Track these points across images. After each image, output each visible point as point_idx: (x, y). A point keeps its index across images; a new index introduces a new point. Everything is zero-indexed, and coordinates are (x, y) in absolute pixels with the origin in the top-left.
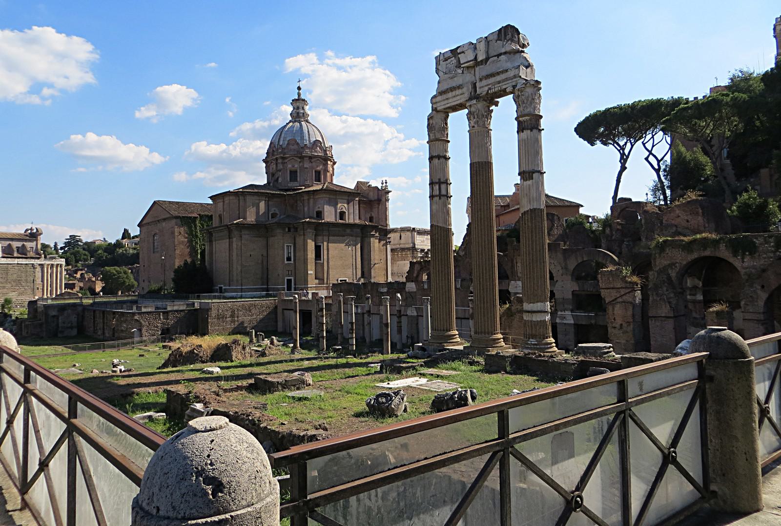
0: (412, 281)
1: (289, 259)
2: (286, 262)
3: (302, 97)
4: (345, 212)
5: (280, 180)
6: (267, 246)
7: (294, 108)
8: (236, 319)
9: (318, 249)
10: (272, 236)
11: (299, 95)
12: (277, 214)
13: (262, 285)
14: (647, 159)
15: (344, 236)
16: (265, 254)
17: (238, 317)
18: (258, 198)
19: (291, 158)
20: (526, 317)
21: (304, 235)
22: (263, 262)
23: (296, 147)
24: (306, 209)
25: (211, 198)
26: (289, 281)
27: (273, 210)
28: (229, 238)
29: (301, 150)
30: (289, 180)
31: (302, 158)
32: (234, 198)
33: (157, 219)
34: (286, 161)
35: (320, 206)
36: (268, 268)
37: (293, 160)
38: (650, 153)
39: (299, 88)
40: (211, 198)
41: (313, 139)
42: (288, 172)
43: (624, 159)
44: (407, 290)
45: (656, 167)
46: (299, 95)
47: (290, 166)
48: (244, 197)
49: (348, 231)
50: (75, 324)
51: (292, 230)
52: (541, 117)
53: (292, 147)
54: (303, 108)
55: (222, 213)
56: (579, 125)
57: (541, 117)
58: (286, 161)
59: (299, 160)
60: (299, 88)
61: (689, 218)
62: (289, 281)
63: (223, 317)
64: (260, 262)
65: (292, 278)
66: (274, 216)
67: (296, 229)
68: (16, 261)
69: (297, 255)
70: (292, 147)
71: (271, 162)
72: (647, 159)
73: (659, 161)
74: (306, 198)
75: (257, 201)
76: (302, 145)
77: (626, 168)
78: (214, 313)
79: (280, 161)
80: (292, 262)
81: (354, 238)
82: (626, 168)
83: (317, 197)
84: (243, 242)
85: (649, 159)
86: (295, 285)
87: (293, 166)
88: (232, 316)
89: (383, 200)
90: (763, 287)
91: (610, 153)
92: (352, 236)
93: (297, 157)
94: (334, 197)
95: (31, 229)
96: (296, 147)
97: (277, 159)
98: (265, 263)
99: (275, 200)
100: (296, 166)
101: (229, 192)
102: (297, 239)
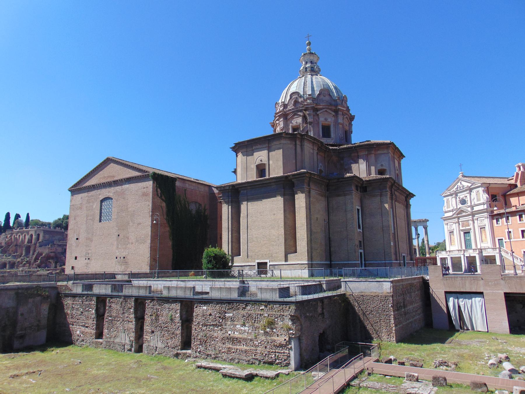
2: (359, 230)
13: (326, 261)
18: (312, 147)
19: (325, 110)
21: (381, 195)
32: (289, 142)
33: (109, 180)
36: (329, 238)
47: (322, 119)
55: (265, 161)
58: (318, 113)
65: (362, 251)
71: (294, 115)
80: (361, 231)
83: (379, 152)
84: (311, 199)
87: (326, 119)
93: (331, 109)
100: (329, 120)
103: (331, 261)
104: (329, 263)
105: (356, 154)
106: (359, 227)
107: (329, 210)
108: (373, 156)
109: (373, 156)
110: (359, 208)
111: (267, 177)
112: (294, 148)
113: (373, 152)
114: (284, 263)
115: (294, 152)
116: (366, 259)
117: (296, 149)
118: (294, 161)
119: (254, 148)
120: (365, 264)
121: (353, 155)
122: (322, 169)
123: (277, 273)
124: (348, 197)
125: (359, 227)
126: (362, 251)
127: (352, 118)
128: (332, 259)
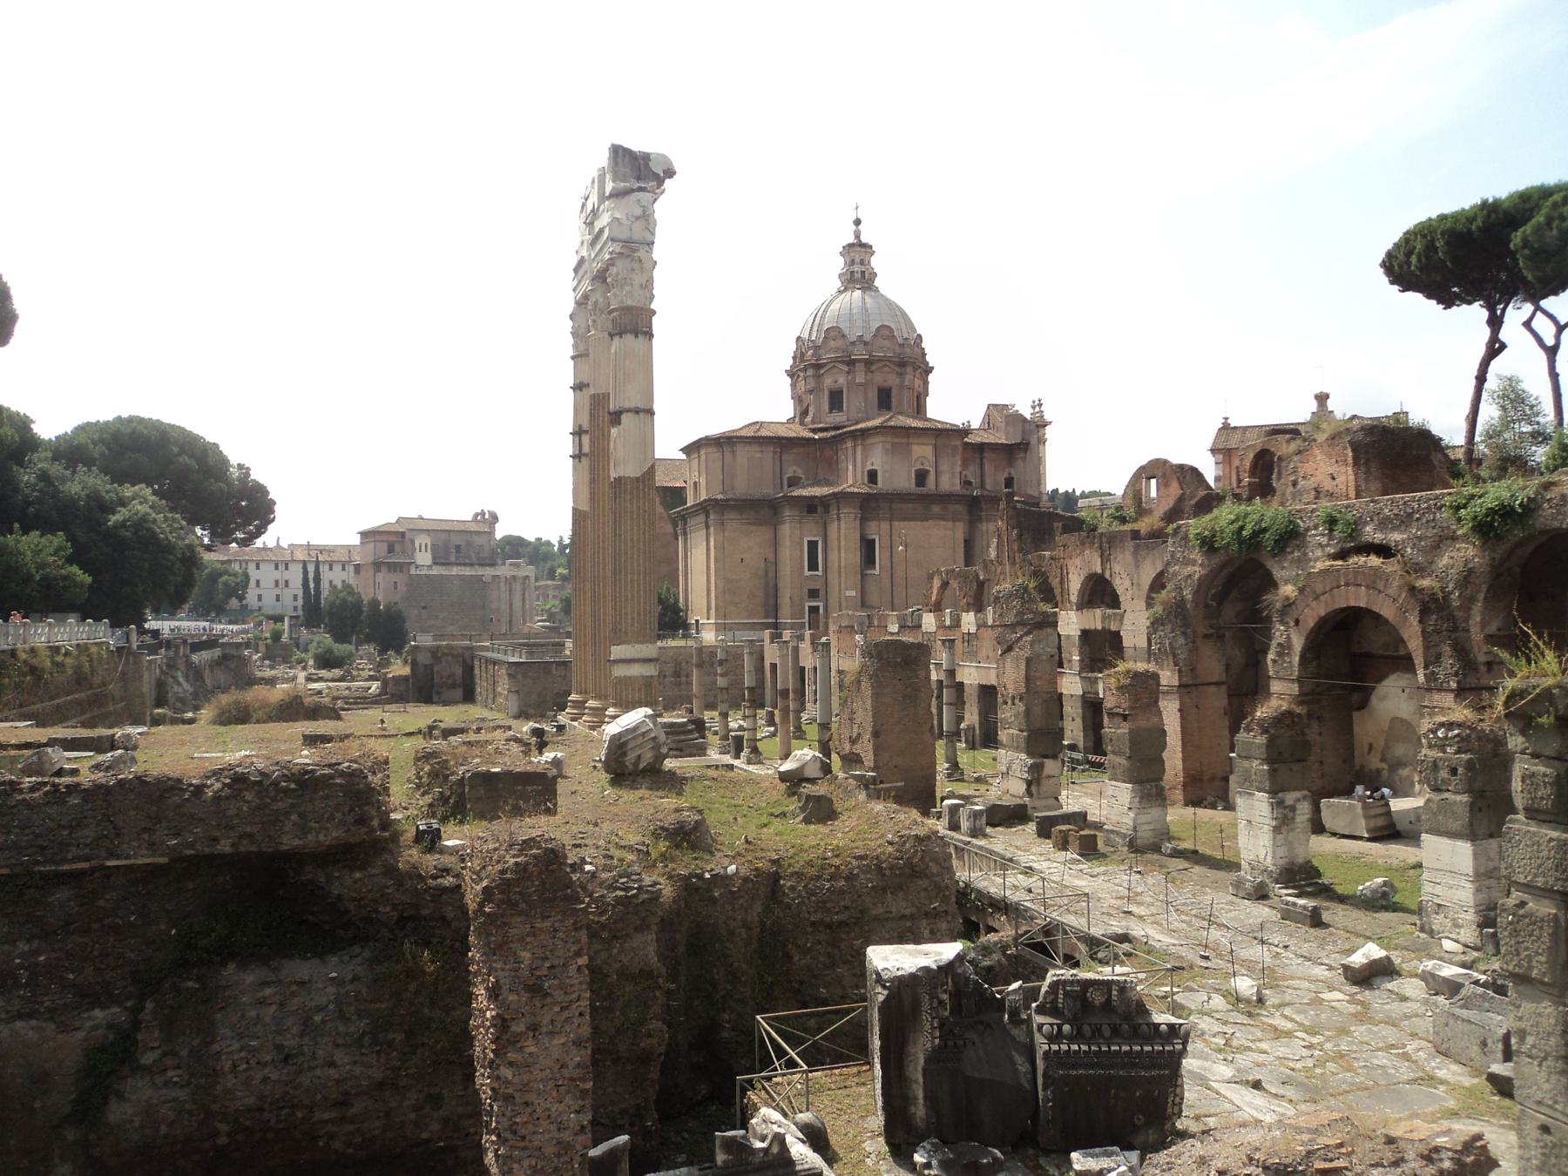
2: (807, 573)
3: (864, 239)
4: (927, 472)
6: (775, 543)
7: (853, 262)
9: (868, 547)
11: (857, 236)
14: (1527, 324)
16: (771, 558)
20: (619, 671)
21: (839, 519)
22: (766, 573)
26: (814, 610)
27: (792, 470)
30: (826, 408)
31: (851, 363)
38: (1538, 308)
39: (857, 222)
41: (875, 325)
42: (826, 393)
43: (1495, 322)
44: (924, 629)
45: (1550, 342)
46: (857, 236)
47: (828, 382)
49: (936, 509)
50: (459, 681)
51: (820, 509)
52: (654, 313)
53: (832, 344)
54: (862, 263)
56: (1389, 255)
57: (654, 313)
60: (857, 222)
61: (1333, 469)
64: (761, 573)
68: (455, 571)
70: (832, 344)
72: (1527, 324)
73: (1560, 328)
74: (849, 444)
75: (758, 455)
76: (853, 339)
77: (1503, 346)
80: (820, 573)
81: (950, 524)
82: (1503, 346)
83: (869, 441)
85: (1534, 324)
89: (1033, 441)
90: (1297, 622)
91: (1474, 315)
92: (943, 519)
95: (483, 513)
96: (839, 343)
98: (771, 575)
102: (833, 528)
106: (813, 566)
122: (800, 473)
125: (813, 566)
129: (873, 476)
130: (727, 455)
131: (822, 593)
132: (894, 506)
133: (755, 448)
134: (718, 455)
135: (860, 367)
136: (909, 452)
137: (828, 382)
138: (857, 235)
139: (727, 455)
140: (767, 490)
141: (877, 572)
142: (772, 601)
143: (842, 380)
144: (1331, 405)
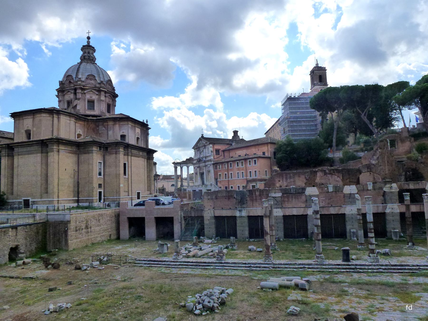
0: (314, 186)
1: (100, 174)
2: (99, 177)
3: (91, 44)
5: (78, 107)
7: (84, 53)
8: (89, 229)
10: (85, 153)
12: (81, 135)
13: (74, 197)
15: (139, 157)
16: (76, 169)
17: (91, 228)
18: (69, 119)
19: (90, 90)
21: (116, 154)
23: (92, 82)
24: (110, 133)
25: (14, 115)
26: (100, 193)
28: (42, 153)
29: (98, 85)
32: (48, 115)
34: (85, 92)
35: (124, 131)
36: (78, 182)
37: (91, 93)
40: (14, 115)
46: (88, 42)
47: (88, 96)
48: (58, 116)
58: (85, 92)
59: (97, 93)
62: (100, 193)
63: (79, 229)
64: (72, 176)
65: (102, 190)
66: (79, 136)
67: (107, 149)
69: (107, 170)
71: (69, 92)
75: (68, 122)
78: (72, 226)
79: (79, 91)
80: (102, 177)
83: (121, 123)
84: (60, 156)
86: (104, 196)
88: (87, 227)
92: (143, 158)
93: (95, 90)
94: (134, 125)
97: (75, 90)
98: (76, 177)
99: (80, 122)
101: (44, 109)
103: (78, 197)
104: (77, 199)
105: (106, 124)
107: (78, 163)
108: (117, 126)
109: (118, 125)
110: (102, 162)
111: (31, 140)
112: (52, 119)
113: (117, 123)
114: (40, 200)
115: (51, 123)
116: (106, 195)
117: (53, 121)
118: (51, 129)
119: (24, 118)
120: (104, 199)
121: (105, 124)
122: (81, 133)
123: (35, 207)
124: (91, 155)
126: (102, 190)
127: (117, 96)
128: (80, 196)
129: (123, 137)
130: (56, 119)
131: (103, 185)
132: (133, 151)
133: (68, 118)
134: (50, 118)
135: (103, 93)
136: (135, 129)
137: (88, 96)
138: (88, 42)
139: (56, 119)
140: (72, 137)
141: (127, 177)
142: (77, 189)
143: (95, 97)
144: (239, 134)
